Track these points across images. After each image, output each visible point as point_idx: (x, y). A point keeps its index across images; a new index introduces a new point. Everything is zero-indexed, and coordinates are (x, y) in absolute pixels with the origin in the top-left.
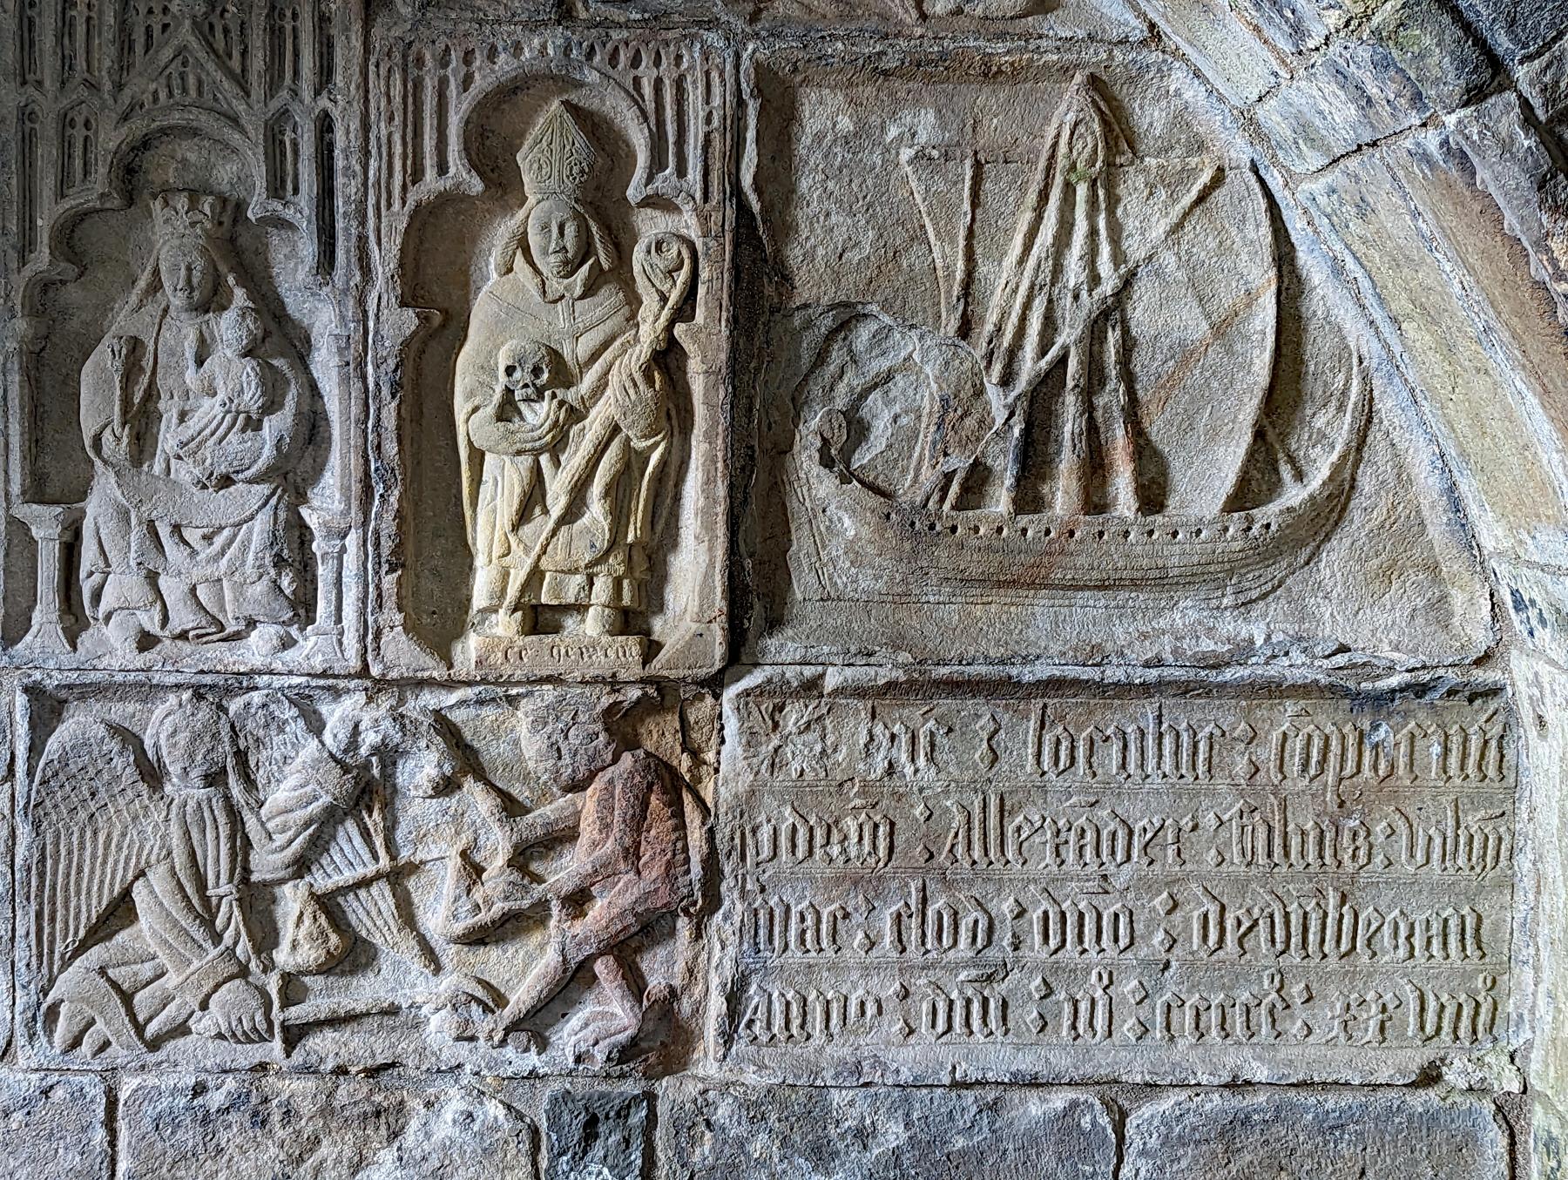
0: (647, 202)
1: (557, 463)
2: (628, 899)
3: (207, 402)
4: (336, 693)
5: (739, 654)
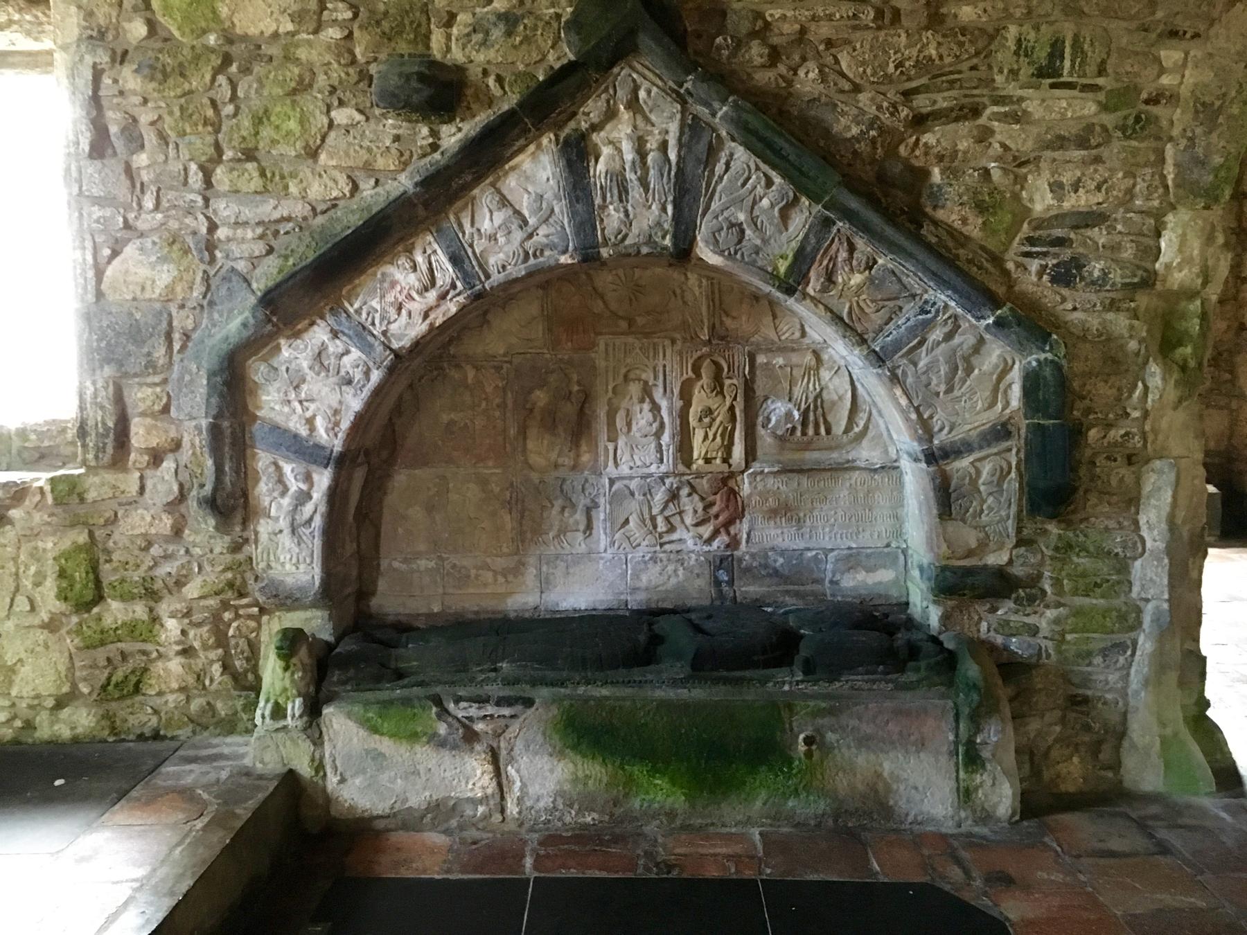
5: (747, 467)
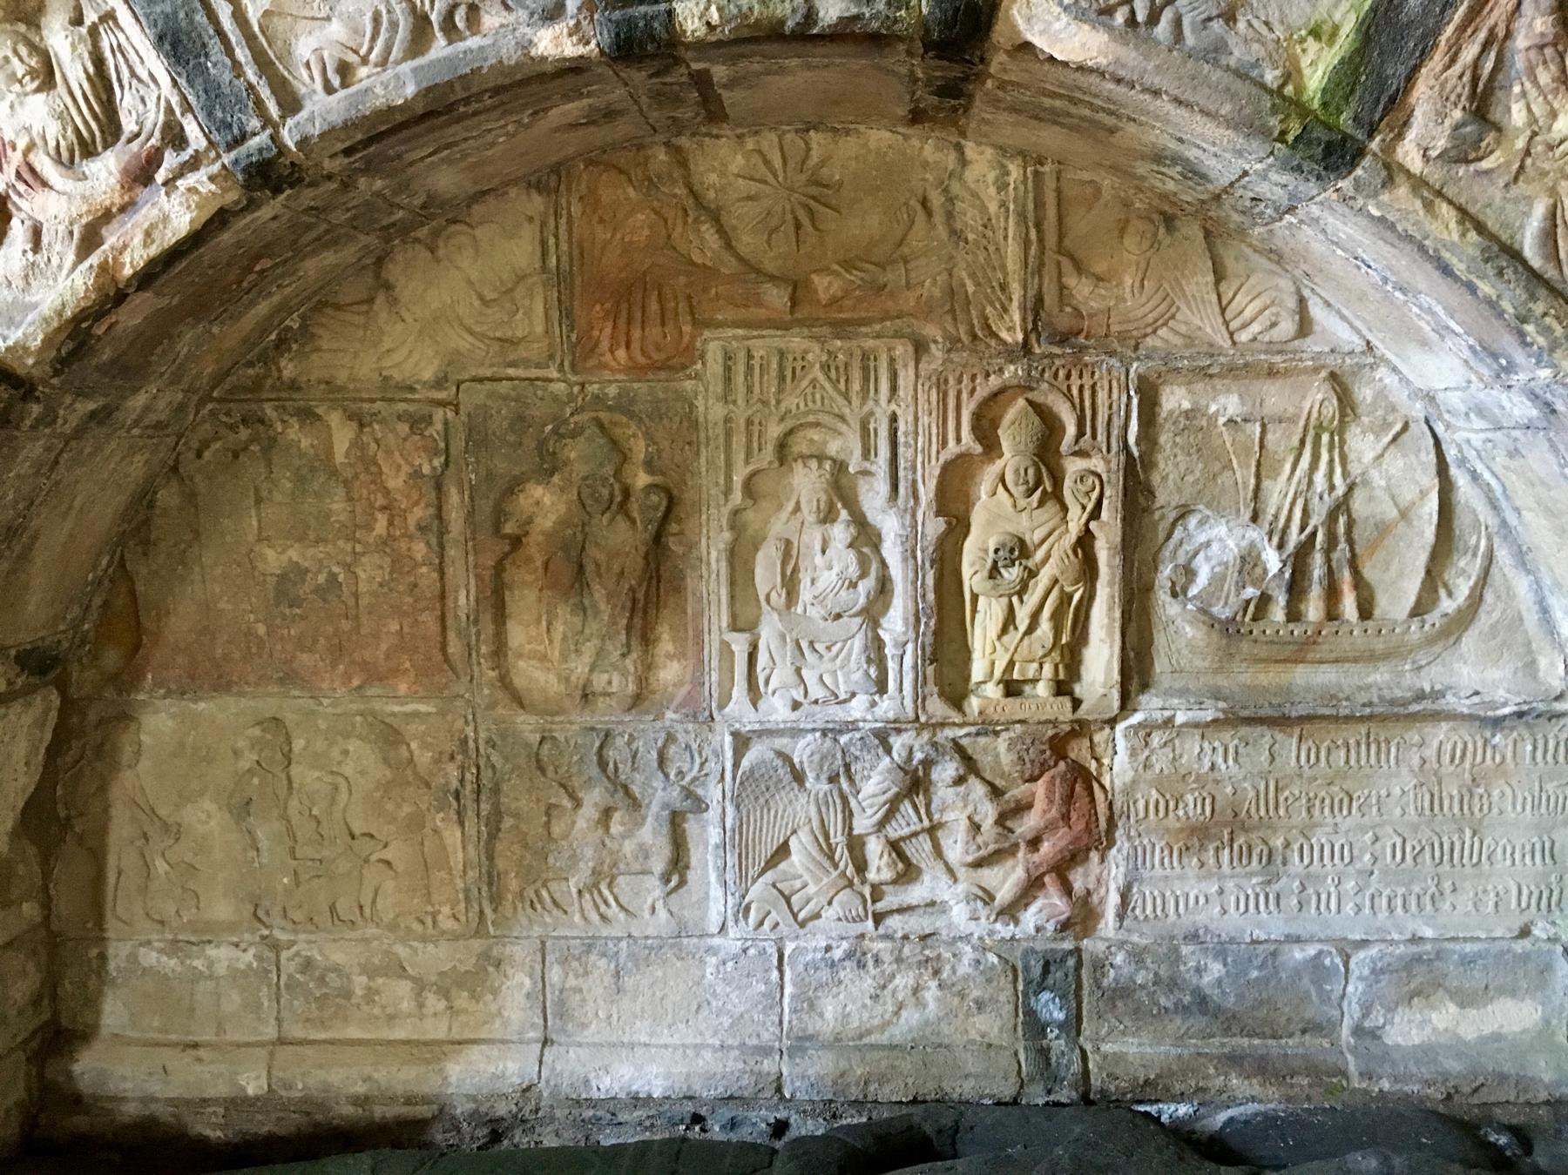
0: (1075, 454)
1: (1022, 601)
2: (1063, 843)
3: (826, 573)
4: (899, 731)
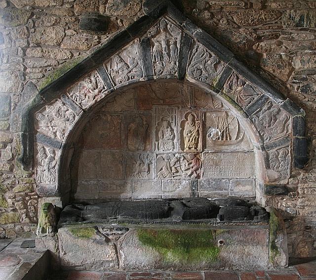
5: (203, 151)
